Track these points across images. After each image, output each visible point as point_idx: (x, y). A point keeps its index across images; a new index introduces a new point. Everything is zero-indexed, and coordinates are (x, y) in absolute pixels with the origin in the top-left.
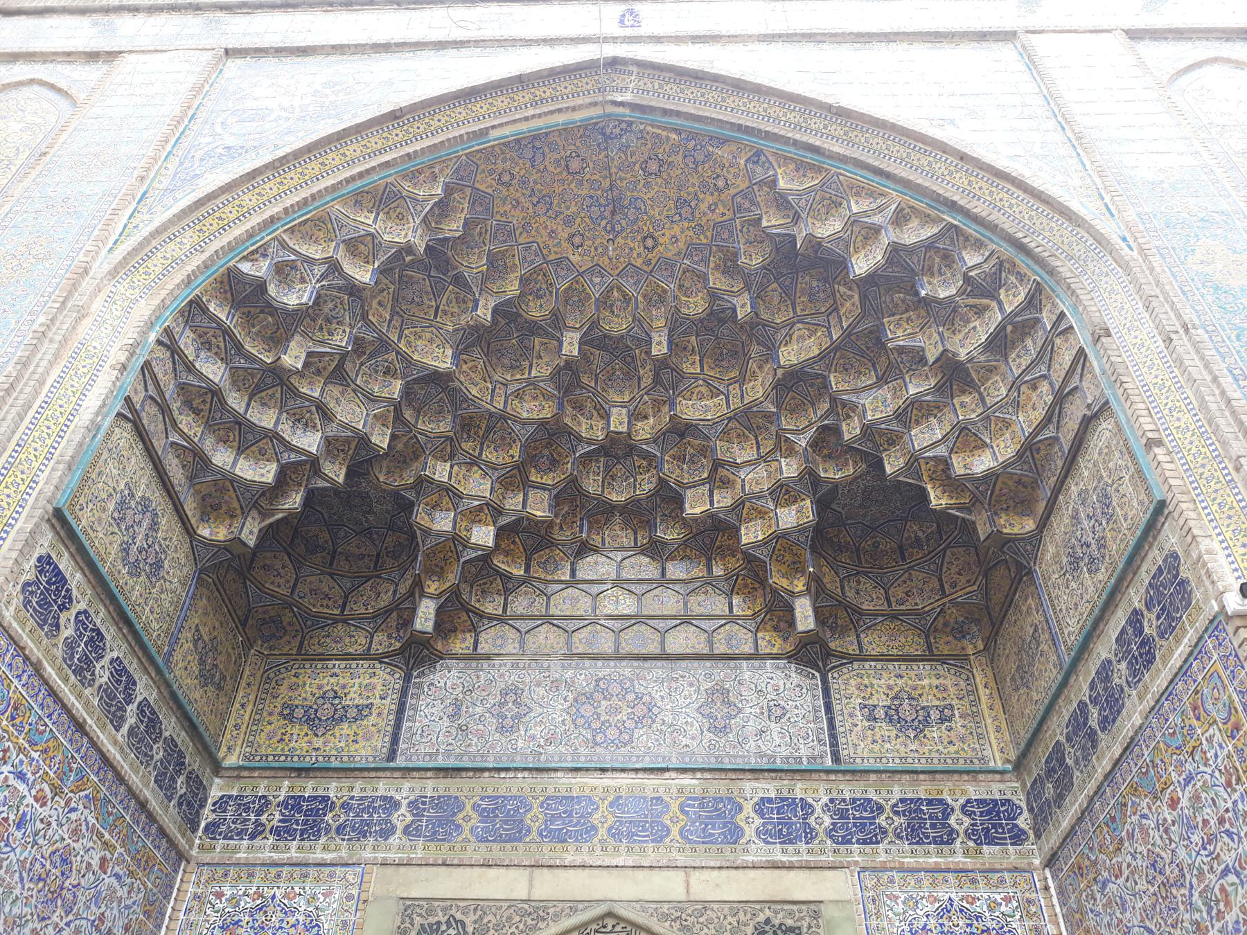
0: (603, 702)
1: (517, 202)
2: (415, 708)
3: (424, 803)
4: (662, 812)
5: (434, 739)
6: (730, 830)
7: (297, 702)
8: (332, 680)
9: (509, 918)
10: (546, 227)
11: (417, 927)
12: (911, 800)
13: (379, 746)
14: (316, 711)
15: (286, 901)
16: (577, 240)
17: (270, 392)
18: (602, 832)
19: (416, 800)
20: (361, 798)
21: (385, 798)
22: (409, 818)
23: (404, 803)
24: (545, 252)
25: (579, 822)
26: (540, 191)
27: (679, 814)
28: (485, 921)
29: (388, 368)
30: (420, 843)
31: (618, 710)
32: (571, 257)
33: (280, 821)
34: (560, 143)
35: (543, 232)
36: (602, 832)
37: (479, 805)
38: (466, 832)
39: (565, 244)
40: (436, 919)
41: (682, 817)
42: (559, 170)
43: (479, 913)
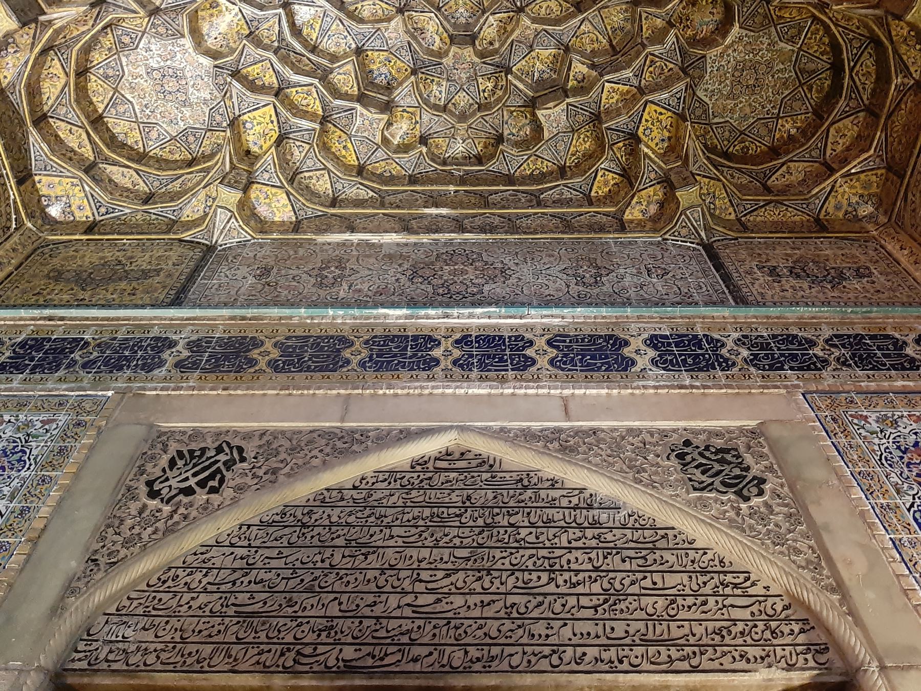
0: (447, 267)
2: (214, 271)
3: (211, 342)
4: (524, 348)
5: (233, 292)
6: (616, 360)
7: (69, 268)
8: (118, 254)
9: (309, 442)
11: (171, 452)
12: (849, 336)
13: (162, 297)
14: (92, 273)
18: (446, 363)
19: (198, 340)
20: (127, 339)
21: (157, 339)
22: (186, 353)
23: (182, 343)
25: (415, 355)
27: (546, 347)
28: (274, 446)
30: (197, 374)
31: (463, 272)
33: (9, 358)
36: (446, 363)
37: (283, 344)
38: (262, 364)
40: (203, 445)
41: (550, 350)
43: (265, 438)
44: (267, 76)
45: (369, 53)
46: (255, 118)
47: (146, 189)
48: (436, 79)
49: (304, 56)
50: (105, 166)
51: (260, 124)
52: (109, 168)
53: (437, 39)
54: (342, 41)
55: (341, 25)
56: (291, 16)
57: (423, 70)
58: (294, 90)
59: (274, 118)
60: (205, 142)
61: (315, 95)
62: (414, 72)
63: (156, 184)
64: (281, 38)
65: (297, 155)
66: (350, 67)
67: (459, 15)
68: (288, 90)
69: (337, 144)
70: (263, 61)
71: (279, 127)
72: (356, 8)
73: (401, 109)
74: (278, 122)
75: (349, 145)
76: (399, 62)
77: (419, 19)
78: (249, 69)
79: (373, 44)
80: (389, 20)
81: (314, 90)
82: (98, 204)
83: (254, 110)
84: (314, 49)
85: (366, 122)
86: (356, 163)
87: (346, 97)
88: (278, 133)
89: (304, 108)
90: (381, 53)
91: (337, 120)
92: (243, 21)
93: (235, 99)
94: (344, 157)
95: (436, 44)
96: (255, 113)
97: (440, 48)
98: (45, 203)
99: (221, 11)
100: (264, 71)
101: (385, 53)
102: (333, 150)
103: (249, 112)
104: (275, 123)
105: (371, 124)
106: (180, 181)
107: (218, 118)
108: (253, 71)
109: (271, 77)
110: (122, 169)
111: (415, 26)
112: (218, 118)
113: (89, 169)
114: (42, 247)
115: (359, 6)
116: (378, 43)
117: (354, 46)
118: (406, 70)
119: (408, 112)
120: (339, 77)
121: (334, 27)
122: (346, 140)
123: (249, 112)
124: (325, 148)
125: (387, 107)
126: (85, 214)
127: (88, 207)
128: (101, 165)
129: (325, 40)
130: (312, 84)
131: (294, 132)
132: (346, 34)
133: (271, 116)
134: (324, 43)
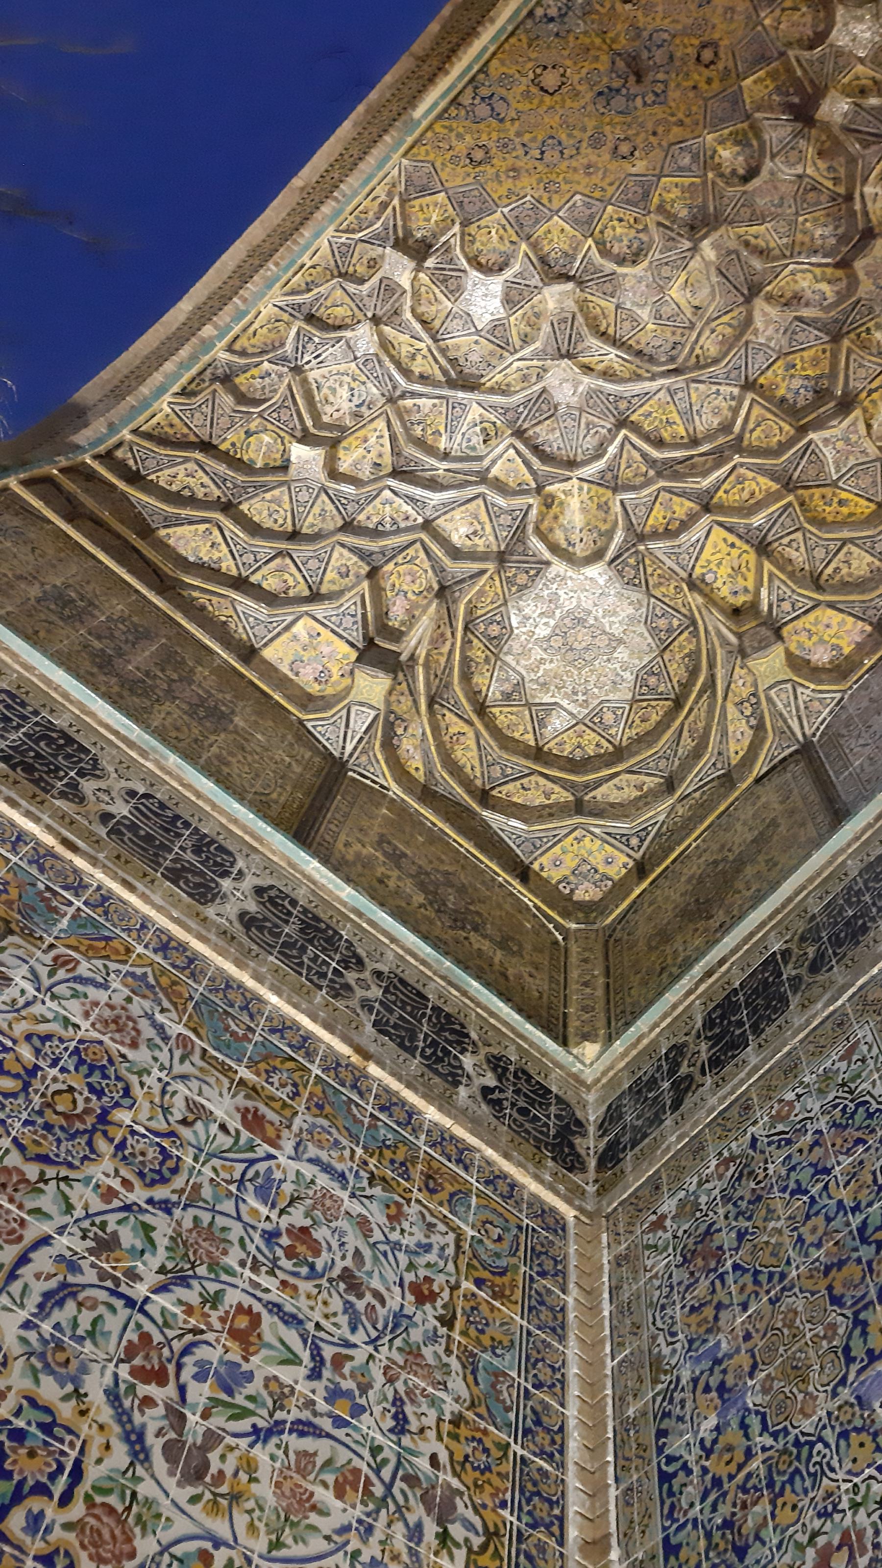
1: (514, 169)
10: (575, 170)
15: (780, 1127)
16: (624, 149)
17: (316, 510)
24: (597, 194)
26: (534, 139)
29: (484, 430)
32: (634, 170)
34: (511, 72)
35: (577, 177)
39: (614, 166)
42: (536, 101)
44: (677, 508)
45: (762, 380)
46: (709, 562)
47: (657, 780)
48: (871, 324)
49: (692, 457)
50: (591, 795)
51: (720, 563)
52: (598, 793)
53: (824, 287)
54: (716, 402)
55: (701, 386)
56: (636, 428)
57: (845, 330)
58: (721, 493)
59: (731, 538)
60: (670, 669)
61: (750, 475)
62: (836, 339)
63: (663, 764)
64: (651, 462)
65: (798, 556)
66: (757, 411)
67: (820, 242)
68: (715, 500)
69: (828, 509)
70: (656, 498)
71: (747, 542)
72: (697, 357)
73: (864, 394)
74: (740, 537)
75: (844, 495)
76: (805, 354)
77: (780, 289)
78: (651, 522)
79: (756, 366)
80: (749, 321)
81: (742, 471)
82: (624, 839)
83: (700, 553)
84: (695, 442)
85: (840, 445)
86: (873, 506)
87: (783, 447)
88: (752, 551)
89: (752, 501)
90: (775, 367)
91: (804, 478)
92: (594, 487)
93: (669, 563)
94: (851, 515)
95: (829, 294)
96: (705, 555)
97: (838, 293)
98: (567, 891)
99: (561, 503)
100: (667, 506)
101: (779, 363)
102: (830, 519)
103: (697, 559)
104: (738, 543)
105: (847, 441)
106: (685, 733)
107: (662, 623)
108: (657, 518)
109: (682, 505)
110: (611, 783)
111: (783, 300)
112: (662, 623)
113: (579, 807)
114: (610, 936)
115: (698, 351)
116: (760, 357)
117: (736, 391)
118: (824, 351)
119: (876, 390)
120: (755, 434)
121: (694, 396)
122: (834, 494)
123: (697, 559)
124: (820, 523)
125: (846, 405)
126: (619, 864)
127: (616, 853)
128: (587, 798)
129: (697, 422)
130: (734, 468)
131: (769, 530)
132: (714, 388)
133: (725, 540)
134: (700, 428)
